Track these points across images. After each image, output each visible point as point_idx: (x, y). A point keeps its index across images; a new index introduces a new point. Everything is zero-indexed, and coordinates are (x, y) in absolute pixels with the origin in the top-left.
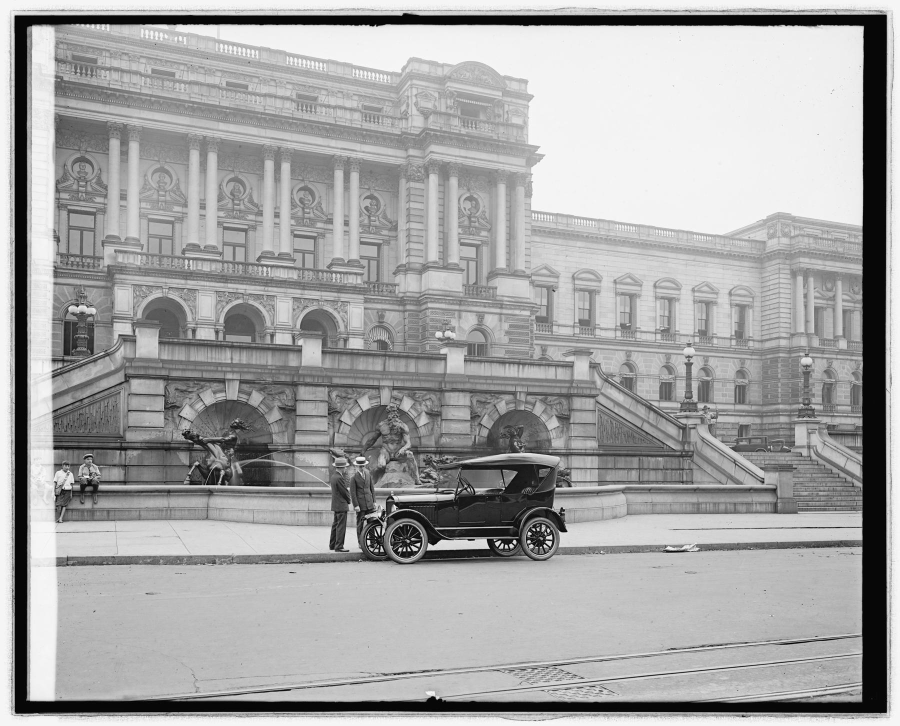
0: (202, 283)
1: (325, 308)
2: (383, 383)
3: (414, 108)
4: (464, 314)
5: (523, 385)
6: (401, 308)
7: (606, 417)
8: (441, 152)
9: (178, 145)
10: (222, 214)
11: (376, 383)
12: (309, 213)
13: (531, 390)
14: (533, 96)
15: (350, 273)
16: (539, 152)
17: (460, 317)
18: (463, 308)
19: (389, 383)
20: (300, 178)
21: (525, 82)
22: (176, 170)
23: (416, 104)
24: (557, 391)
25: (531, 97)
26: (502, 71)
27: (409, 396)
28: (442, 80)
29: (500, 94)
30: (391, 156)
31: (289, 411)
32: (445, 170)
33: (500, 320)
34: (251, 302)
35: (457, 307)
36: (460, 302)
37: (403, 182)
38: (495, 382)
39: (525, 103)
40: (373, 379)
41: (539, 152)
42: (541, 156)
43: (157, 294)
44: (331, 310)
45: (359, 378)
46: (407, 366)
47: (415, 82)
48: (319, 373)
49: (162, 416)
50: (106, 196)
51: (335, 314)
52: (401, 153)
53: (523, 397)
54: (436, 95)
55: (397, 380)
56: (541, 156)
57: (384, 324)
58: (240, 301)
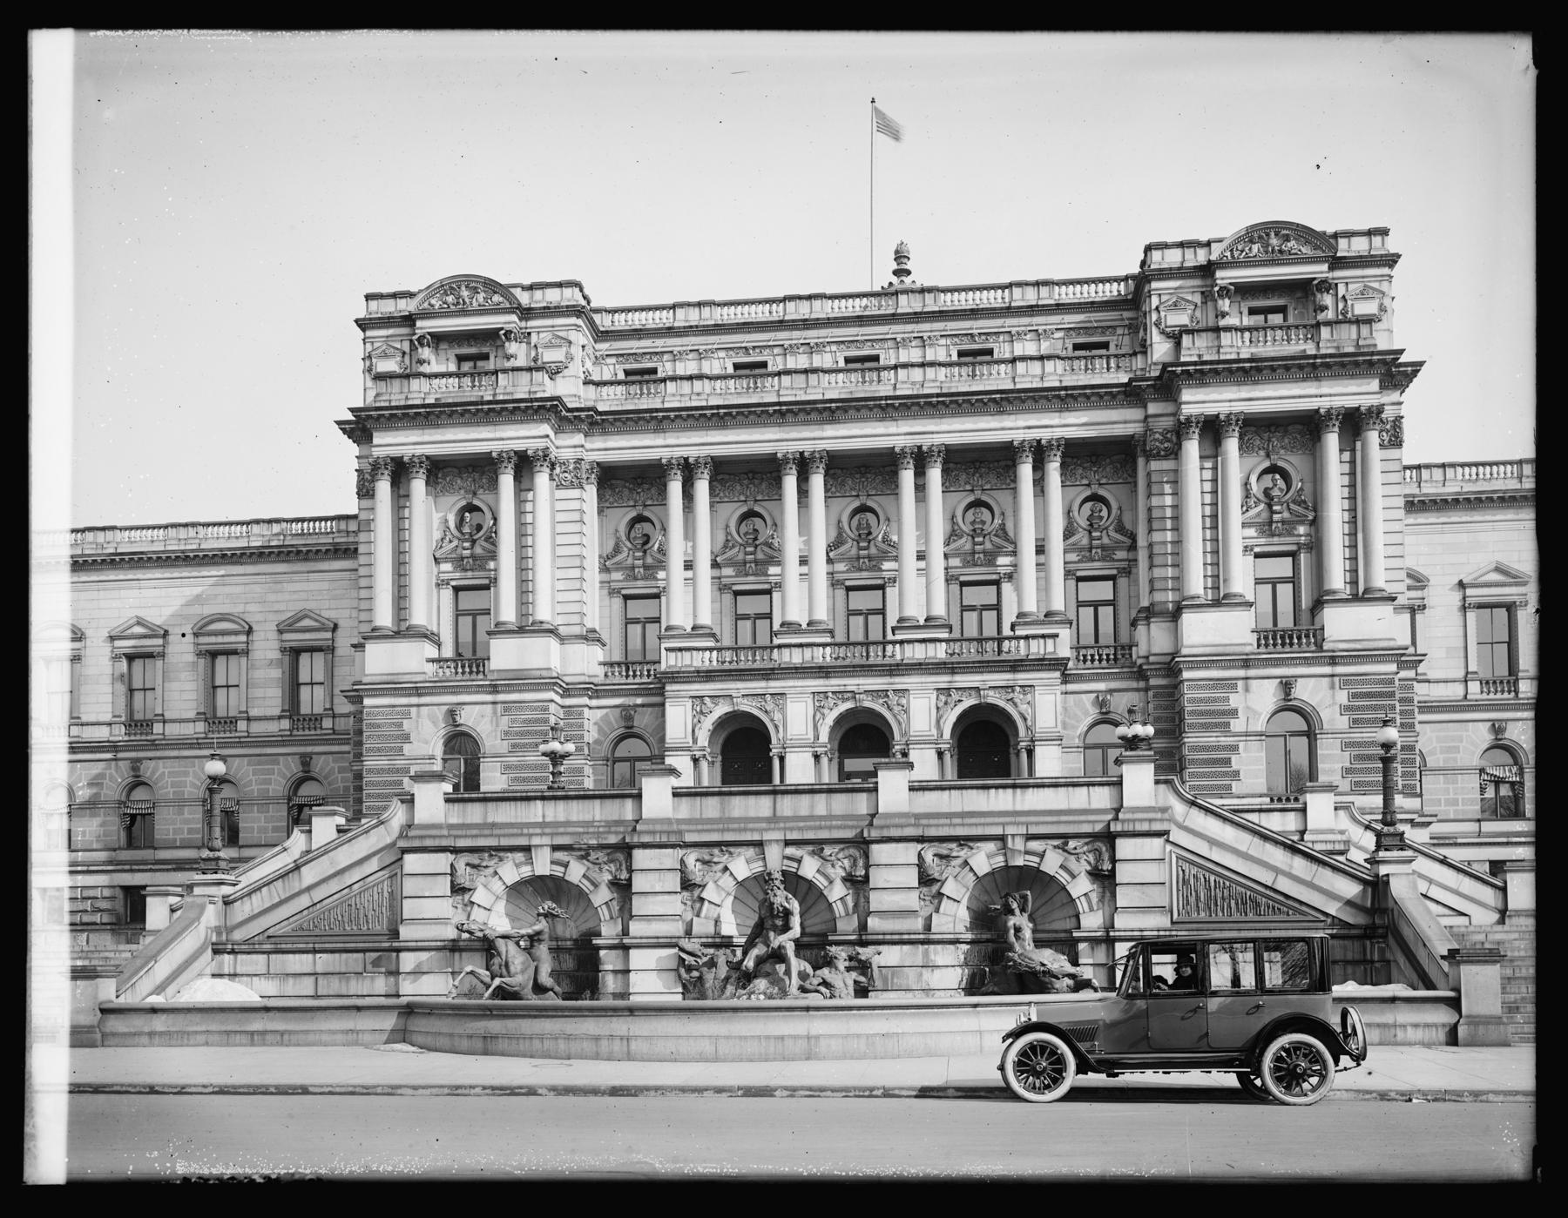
0: (791, 683)
1: (990, 700)
2: (767, 836)
3: (1155, 331)
4: (1253, 683)
5: (1018, 824)
6: (1142, 684)
7: (1194, 870)
8: (1198, 401)
9: (994, 463)
10: (1073, 557)
11: (756, 837)
12: (1100, 538)
13: (1034, 830)
14: (1399, 256)
15: (1034, 637)
16: (1403, 359)
17: (1247, 690)
18: (1252, 672)
19: (779, 835)
20: (968, 487)
21: (1384, 232)
22: (999, 499)
23: (1157, 324)
24: (1087, 829)
25: (1391, 260)
26: (1318, 228)
27: (813, 853)
28: (1207, 270)
29: (1325, 267)
30: (1118, 422)
31: (623, 889)
32: (1213, 429)
33: (1332, 687)
34: (868, 704)
35: (1241, 673)
36: (1246, 663)
37: (1141, 461)
38: (751, 826)
39: (1386, 271)
40: (752, 830)
41: (1403, 359)
42: (1417, 366)
43: (722, 709)
44: (1002, 704)
45: (728, 830)
46: (828, 804)
47: (1154, 285)
48: (665, 828)
49: (915, 894)
50: (1014, 553)
51: (1009, 708)
52: (1135, 414)
53: (1019, 844)
54: (1197, 299)
55: (791, 829)
56: (1417, 366)
57: (1111, 716)
58: (849, 705)
